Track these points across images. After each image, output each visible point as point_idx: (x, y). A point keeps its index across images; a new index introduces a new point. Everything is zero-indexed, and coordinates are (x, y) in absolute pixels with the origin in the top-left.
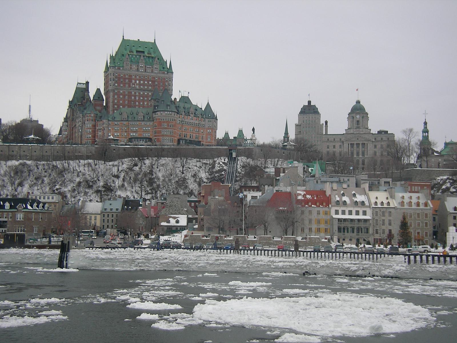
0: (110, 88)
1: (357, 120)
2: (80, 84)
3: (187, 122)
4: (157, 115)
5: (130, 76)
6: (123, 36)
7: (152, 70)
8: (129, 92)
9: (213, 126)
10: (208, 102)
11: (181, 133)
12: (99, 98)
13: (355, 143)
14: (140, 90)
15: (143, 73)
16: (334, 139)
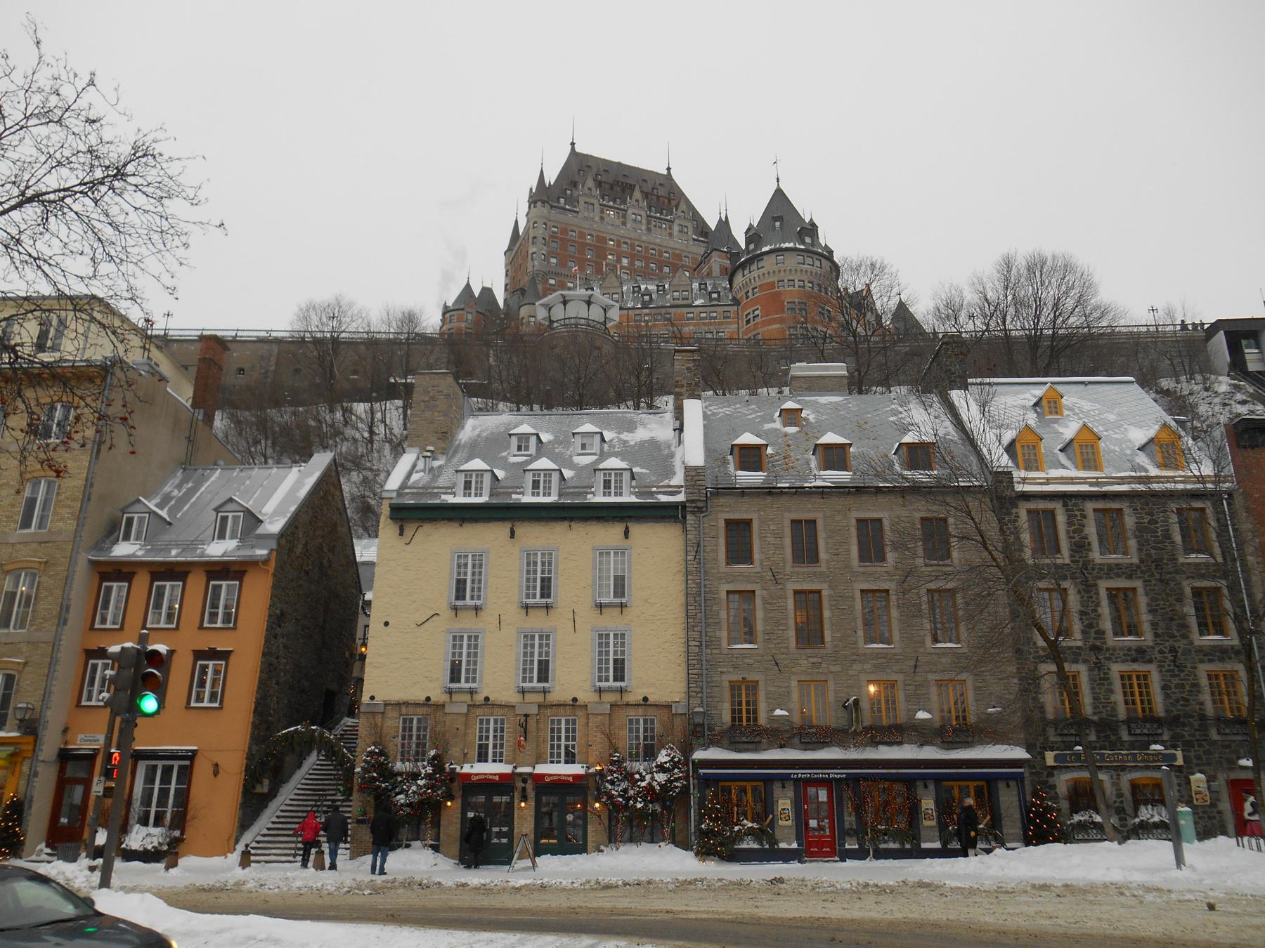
4: (755, 274)
5: (603, 240)
6: (573, 144)
15: (644, 238)
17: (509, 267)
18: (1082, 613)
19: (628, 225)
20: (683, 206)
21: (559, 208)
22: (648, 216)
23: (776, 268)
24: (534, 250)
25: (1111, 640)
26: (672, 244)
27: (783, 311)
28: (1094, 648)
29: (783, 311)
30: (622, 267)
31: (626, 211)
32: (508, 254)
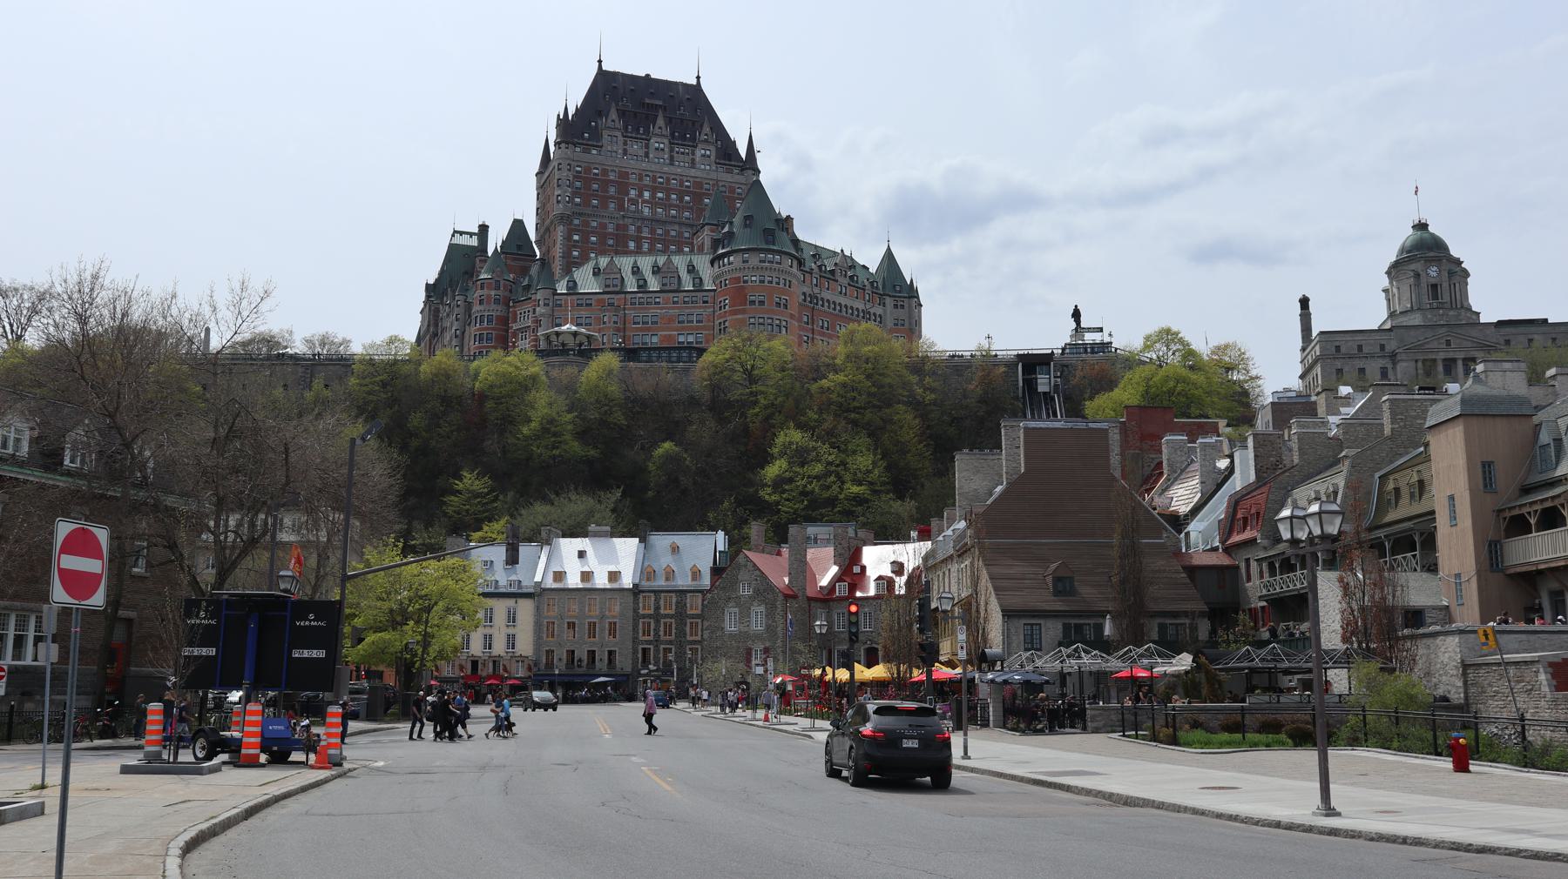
0: (558, 209)
1: (1433, 281)
2: (461, 233)
3: (828, 301)
4: (726, 268)
5: (624, 175)
6: (600, 61)
7: (693, 160)
8: (618, 227)
9: (910, 324)
10: (889, 249)
11: (811, 336)
12: (519, 247)
13: (1442, 356)
14: (654, 221)
15: (666, 169)
16: (1360, 348)
17: (540, 191)
18: (654, 630)
19: (651, 156)
20: (706, 129)
21: (583, 144)
22: (670, 143)
23: (741, 265)
24: (559, 192)
25: (662, 638)
26: (693, 172)
27: (745, 304)
28: (656, 641)
29: (745, 304)
30: (644, 202)
31: (649, 140)
32: (539, 176)
